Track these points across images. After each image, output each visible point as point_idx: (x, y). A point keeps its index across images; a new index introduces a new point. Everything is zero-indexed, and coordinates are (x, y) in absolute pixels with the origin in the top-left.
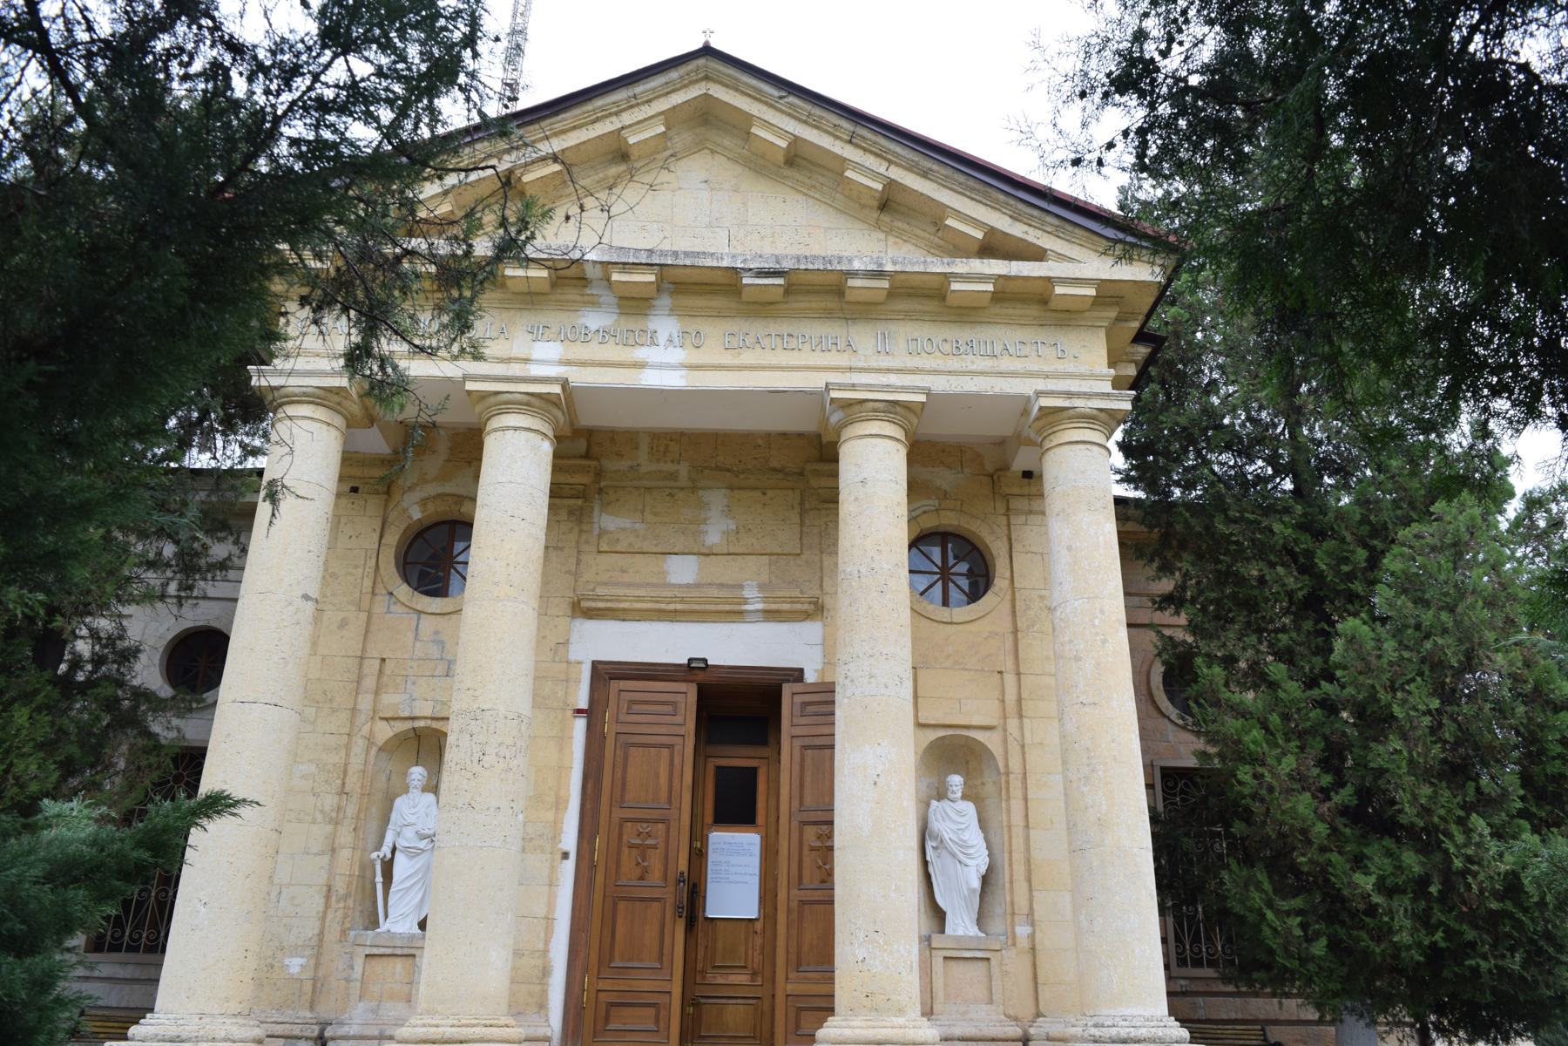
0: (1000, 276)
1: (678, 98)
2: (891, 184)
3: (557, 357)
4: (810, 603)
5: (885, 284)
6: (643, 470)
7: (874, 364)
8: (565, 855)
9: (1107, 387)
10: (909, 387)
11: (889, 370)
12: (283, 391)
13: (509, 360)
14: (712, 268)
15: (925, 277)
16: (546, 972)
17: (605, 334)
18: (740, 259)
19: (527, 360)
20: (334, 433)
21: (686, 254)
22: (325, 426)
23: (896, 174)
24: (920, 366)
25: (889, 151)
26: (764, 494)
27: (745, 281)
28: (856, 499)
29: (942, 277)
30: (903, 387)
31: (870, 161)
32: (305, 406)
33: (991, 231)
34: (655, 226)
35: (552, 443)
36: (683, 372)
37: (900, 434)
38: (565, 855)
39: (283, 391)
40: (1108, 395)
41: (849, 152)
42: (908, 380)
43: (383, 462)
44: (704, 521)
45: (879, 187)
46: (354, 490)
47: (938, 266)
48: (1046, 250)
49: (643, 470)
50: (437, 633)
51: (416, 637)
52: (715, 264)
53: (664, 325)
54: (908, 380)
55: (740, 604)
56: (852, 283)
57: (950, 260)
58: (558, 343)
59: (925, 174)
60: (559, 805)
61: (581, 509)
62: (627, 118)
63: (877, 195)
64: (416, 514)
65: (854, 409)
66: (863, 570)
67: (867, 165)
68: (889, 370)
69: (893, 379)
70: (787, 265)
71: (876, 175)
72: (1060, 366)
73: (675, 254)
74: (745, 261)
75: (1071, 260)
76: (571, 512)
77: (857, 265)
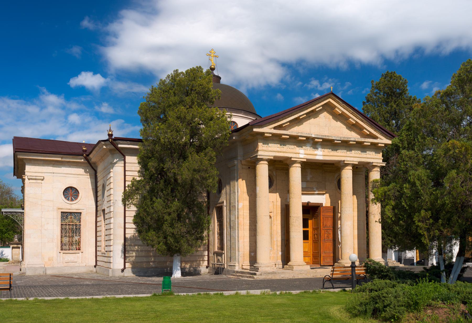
2: (356, 122)
3: (304, 153)
21: (328, 136)
28: (347, 180)
46: (249, 168)
47: (363, 140)
59: (362, 121)
74: (336, 138)
75: (381, 139)
77: (352, 139)
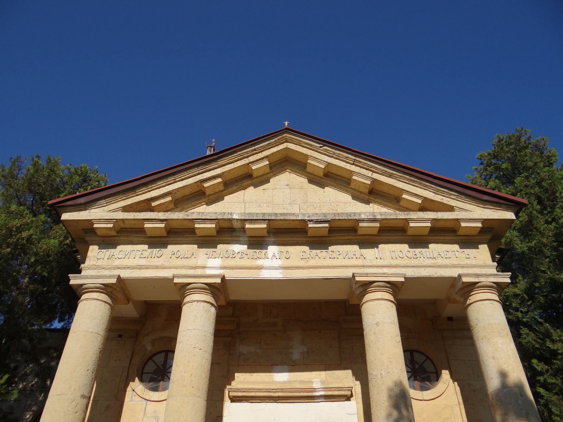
0: (433, 219)
2: (374, 181)
4: (349, 390)
5: (377, 225)
7: (376, 264)
9: (494, 271)
10: (395, 274)
11: (383, 266)
12: (84, 286)
13: (196, 268)
14: (294, 220)
15: (396, 221)
17: (242, 255)
18: (307, 215)
19: (204, 267)
20: (108, 306)
21: (281, 214)
22: (103, 303)
23: (376, 176)
24: (398, 264)
25: (372, 167)
26: (320, 332)
27: (310, 226)
28: (375, 333)
29: (405, 221)
30: (392, 274)
31: (364, 172)
32: (95, 293)
33: (425, 199)
34: (265, 205)
35: (216, 309)
36: (281, 271)
37: (392, 298)
39: (84, 286)
40: (497, 275)
41: (353, 168)
42: (393, 271)
43: (133, 321)
45: (369, 183)
46: (120, 336)
47: (402, 215)
48: (453, 207)
50: (155, 412)
51: (144, 414)
52: (295, 218)
53: (272, 249)
54: (393, 271)
55: (312, 392)
56: (361, 225)
57: (407, 213)
58: (220, 259)
59: (390, 176)
62: (252, 159)
63: (368, 186)
64: (149, 348)
65: (366, 286)
66: (383, 373)
67: (362, 173)
68: (383, 266)
69: (385, 270)
70: (329, 218)
71: (367, 177)
72: (468, 262)
73: (276, 214)
77: (363, 216)
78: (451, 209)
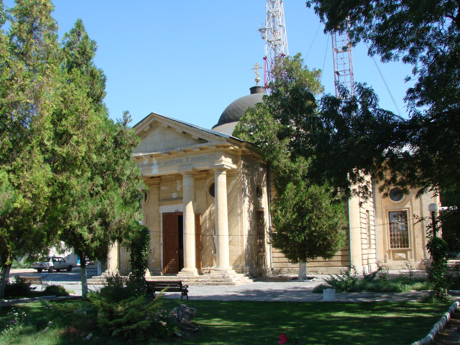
1: (150, 121)
6: (168, 178)
8: (161, 244)
16: (160, 261)
38: (161, 244)
44: (177, 186)
49: (168, 178)
60: (160, 237)
61: (159, 186)
62: (143, 127)
75: (210, 142)
76: (157, 187)
78: (206, 141)
